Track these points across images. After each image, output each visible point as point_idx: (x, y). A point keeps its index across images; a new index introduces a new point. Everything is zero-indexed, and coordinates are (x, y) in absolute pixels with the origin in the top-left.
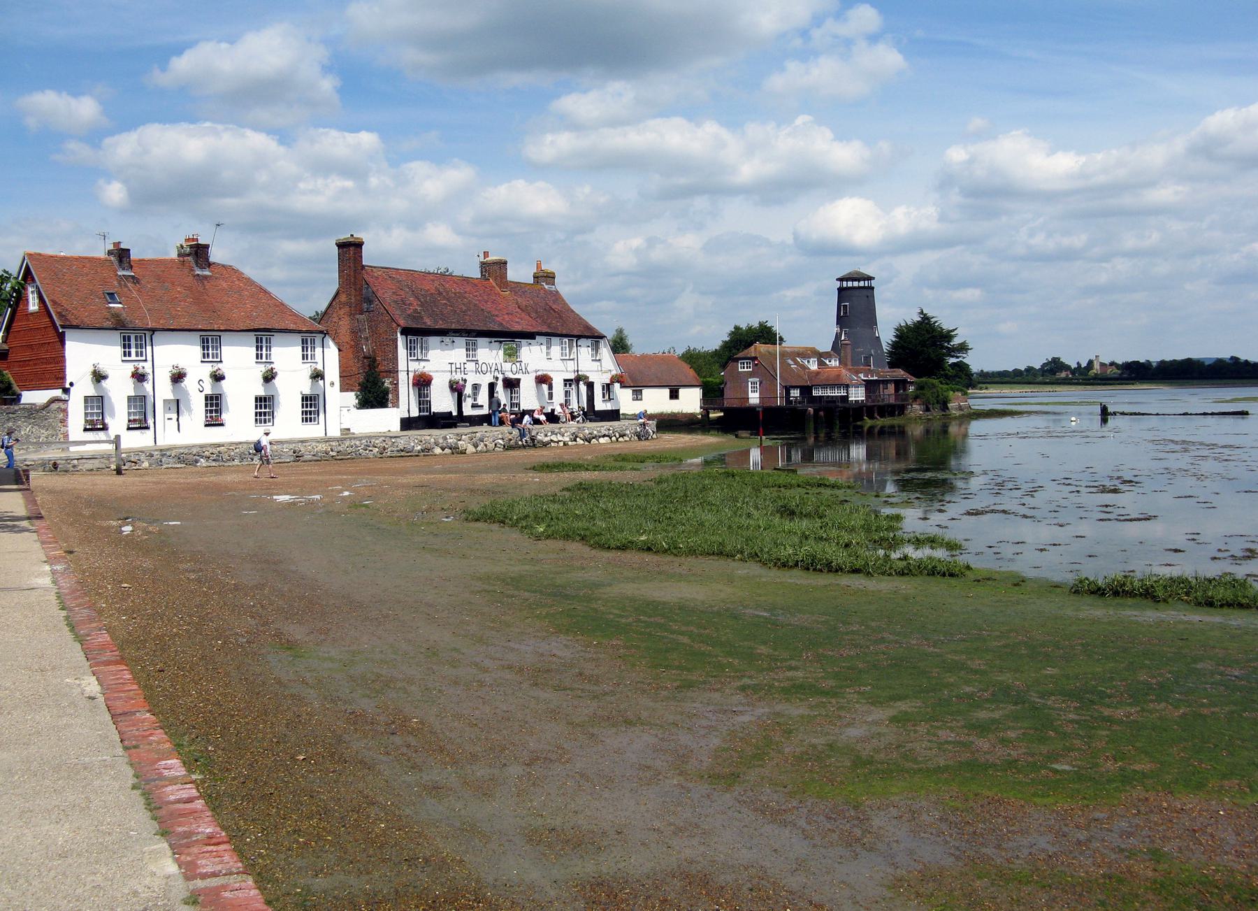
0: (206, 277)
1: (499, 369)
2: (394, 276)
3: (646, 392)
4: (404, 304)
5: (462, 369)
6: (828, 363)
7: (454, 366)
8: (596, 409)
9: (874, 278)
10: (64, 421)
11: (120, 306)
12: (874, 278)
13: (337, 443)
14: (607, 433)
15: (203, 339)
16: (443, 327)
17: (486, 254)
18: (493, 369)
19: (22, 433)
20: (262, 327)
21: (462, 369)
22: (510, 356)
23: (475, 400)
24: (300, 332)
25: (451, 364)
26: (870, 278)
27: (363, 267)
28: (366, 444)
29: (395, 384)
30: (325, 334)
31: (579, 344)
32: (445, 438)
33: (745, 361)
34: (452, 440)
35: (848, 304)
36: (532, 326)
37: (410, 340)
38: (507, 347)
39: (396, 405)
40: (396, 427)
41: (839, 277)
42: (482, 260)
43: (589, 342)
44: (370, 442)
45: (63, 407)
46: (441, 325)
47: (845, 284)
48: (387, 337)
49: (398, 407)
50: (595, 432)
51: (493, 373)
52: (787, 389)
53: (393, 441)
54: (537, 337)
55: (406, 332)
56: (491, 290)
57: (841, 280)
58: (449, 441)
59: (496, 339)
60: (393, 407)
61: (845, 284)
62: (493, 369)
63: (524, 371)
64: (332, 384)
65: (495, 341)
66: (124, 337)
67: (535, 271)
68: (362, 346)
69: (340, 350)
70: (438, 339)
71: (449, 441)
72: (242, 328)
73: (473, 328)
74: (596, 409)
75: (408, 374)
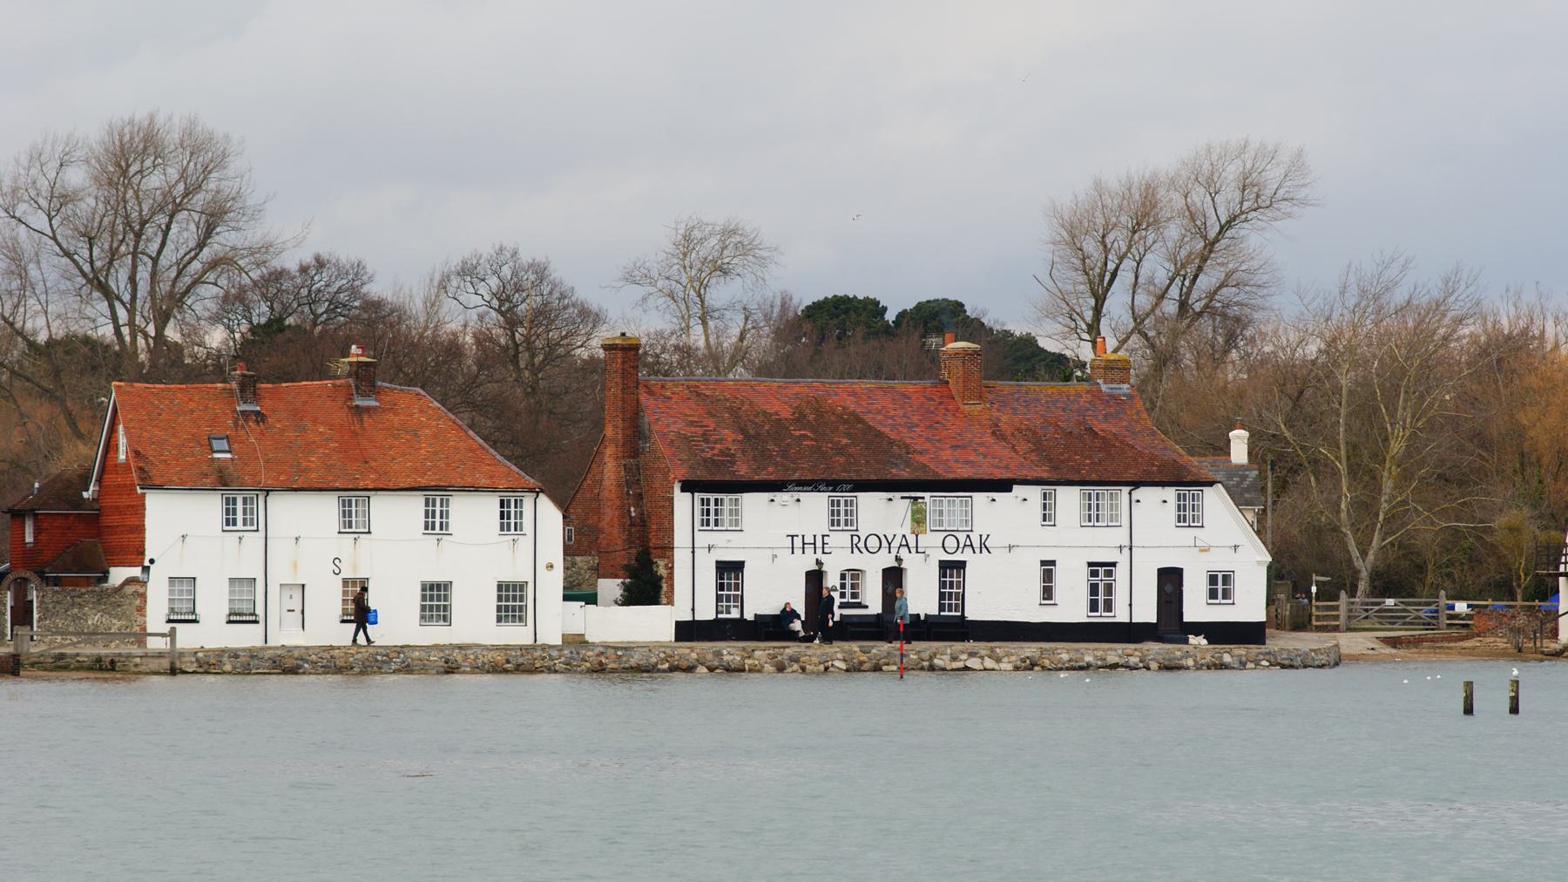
0: (368, 409)
1: (912, 544)
2: (708, 393)
4: (706, 441)
5: (819, 544)
10: (141, 610)
11: (228, 456)
14: (1121, 661)
15: (344, 501)
16: (772, 477)
18: (895, 544)
19: (90, 622)
20: (433, 483)
21: (819, 544)
22: (918, 523)
23: (854, 595)
24: (494, 490)
25: (792, 536)
28: (569, 655)
30: (538, 493)
32: (718, 654)
34: (732, 657)
36: (1007, 467)
39: (670, 602)
40: (669, 634)
43: (1170, 493)
44: (578, 653)
45: (141, 590)
49: (673, 605)
51: (894, 551)
53: (620, 653)
54: (1014, 486)
55: (688, 487)
58: (725, 658)
60: (668, 604)
62: (895, 544)
63: (976, 544)
65: (902, 498)
66: (227, 499)
68: (629, 508)
69: (564, 517)
71: (725, 658)
72: (402, 485)
73: (844, 476)
75: (693, 552)
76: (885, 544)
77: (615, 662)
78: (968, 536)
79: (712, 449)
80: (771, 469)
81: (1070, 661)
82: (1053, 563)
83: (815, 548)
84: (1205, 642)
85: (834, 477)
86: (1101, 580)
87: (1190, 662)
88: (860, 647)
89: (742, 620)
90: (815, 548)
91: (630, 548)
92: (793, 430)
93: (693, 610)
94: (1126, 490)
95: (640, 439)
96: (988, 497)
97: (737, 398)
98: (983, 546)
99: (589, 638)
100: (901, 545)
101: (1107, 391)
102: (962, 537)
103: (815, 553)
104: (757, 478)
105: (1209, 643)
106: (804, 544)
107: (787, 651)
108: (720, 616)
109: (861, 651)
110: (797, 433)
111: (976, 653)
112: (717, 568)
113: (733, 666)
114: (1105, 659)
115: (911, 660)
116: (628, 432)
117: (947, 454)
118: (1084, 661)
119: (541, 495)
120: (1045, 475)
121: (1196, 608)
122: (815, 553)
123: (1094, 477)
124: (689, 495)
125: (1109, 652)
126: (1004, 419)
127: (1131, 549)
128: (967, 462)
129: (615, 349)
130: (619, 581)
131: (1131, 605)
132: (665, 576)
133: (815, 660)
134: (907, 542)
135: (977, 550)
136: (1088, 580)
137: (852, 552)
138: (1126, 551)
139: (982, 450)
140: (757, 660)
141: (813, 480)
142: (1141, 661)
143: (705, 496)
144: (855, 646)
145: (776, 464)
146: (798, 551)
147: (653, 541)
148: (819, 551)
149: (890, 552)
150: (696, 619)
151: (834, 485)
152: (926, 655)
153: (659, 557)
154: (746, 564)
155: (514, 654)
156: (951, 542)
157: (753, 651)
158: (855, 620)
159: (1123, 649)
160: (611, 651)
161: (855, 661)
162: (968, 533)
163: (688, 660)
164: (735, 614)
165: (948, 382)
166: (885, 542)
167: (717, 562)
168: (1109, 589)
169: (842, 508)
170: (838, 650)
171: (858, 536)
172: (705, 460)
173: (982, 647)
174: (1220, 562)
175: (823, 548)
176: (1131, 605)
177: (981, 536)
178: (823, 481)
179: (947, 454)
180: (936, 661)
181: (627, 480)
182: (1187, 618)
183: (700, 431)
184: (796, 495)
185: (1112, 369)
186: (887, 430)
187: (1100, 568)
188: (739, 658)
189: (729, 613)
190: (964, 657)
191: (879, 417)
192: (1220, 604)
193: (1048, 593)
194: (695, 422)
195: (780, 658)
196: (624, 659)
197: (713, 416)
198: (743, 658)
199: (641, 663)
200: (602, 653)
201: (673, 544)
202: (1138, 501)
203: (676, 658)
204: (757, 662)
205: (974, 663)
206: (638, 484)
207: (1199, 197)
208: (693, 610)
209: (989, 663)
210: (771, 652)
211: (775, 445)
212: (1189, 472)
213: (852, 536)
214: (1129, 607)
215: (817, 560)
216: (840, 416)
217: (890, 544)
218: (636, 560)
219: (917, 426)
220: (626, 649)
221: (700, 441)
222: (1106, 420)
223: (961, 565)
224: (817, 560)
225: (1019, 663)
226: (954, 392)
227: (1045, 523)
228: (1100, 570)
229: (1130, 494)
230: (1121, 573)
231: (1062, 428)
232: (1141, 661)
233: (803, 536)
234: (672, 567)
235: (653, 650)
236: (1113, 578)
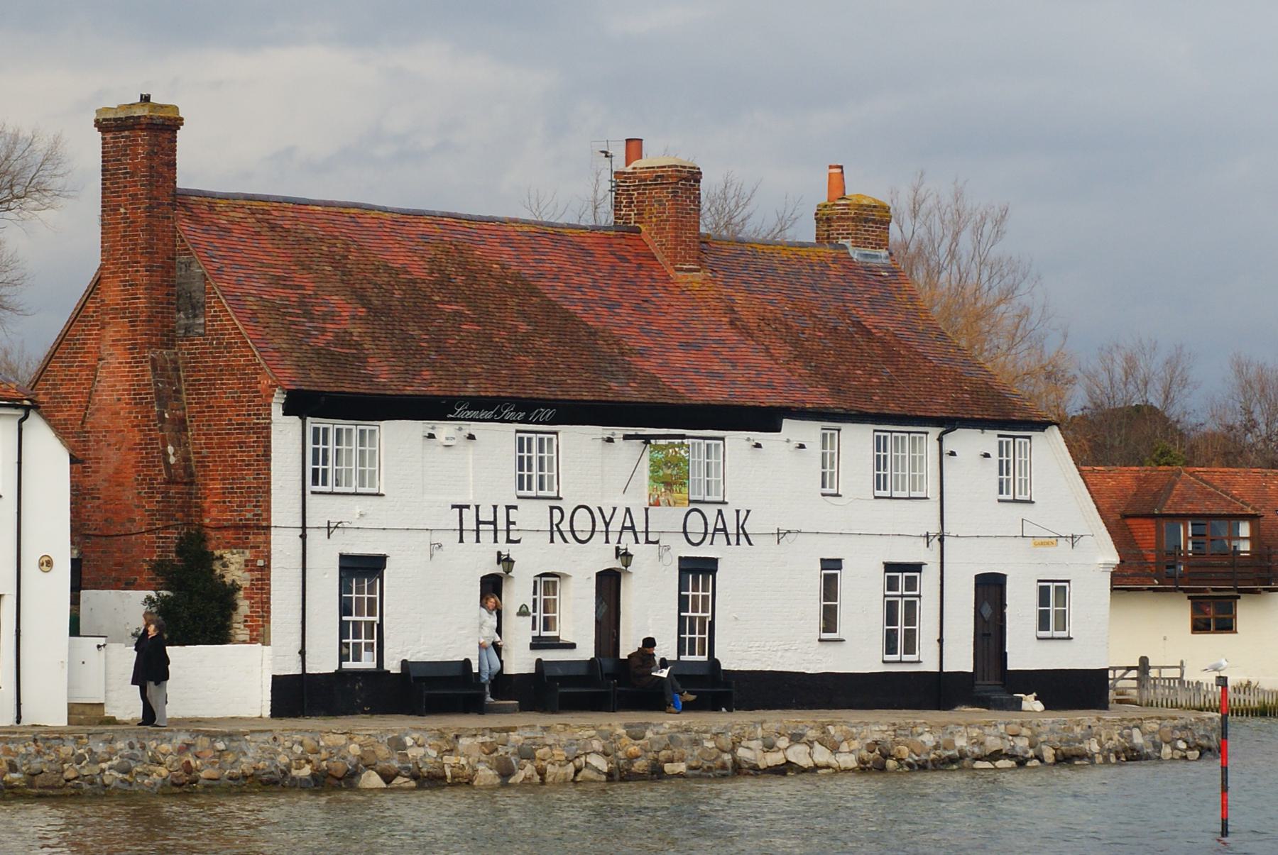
1: (640, 527)
4: (310, 316)
5: (502, 524)
7: (469, 515)
13: (32, 749)
14: (1006, 746)
16: (434, 390)
18: (616, 526)
21: (502, 524)
22: (668, 484)
23: (548, 624)
25: (461, 507)
27: (182, 200)
28: (127, 752)
29: (261, 569)
30: (27, 409)
31: (947, 449)
32: (398, 745)
34: (421, 751)
36: (770, 386)
37: (316, 430)
39: (260, 635)
40: (259, 702)
42: (620, 164)
43: (988, 440)
44: (143, 747)
46: (426, 384)
48: (241, 419)
49: (266, 643)
50: (961, 742)
51: (613, 538)
53: (220, 745)
55: (298, 405)
56: (640, 266)
58: (413, 753)
59: (631, 431)
60: (253, 640)
62: (616, 526)
63: (732, 529)
64: (47, 563)
65: (626, 437)
67: (824, 200)
68: (165, 446)
69: (73, 460)
70: (412, 430)
71: (413, 753)
73: (542, 392)
75: (303, 537)
76: (600, 525)
77: (213, 764)
78: (720, 512)
79: (323, 331)
80: (427, 374)
81: (936, 747)
83: (496, 531)
84: (1039, 706)
86: (902, 596)
87: (1095, 747)
88: (626, 726)
89: (379, 675)
90: (496, 531)
91: (167, 527)
92: (442, 302)
93: (302, 653)
94: (934, 432)
95: (179, 311)
96: (748, 439)
97: (336, 238)
98: (741, 531)
99: (117, 718)
100: (624, 528)
101: (861, 259)
102: (711, 512)
103: (496, 541)
104: (409, 390)
105: (1047, 707)
106: (479, 522)
107: (514, 737)
108: (349, 665)
109: (628, 733)
111: (802, 736)
112: (341, 568)
113: (424, 770)
114: (982, 744)
115: (705, 749)
116: (158, 295)
118: (955, 747)
119: (32, 414)
120: (830, 403)
122: (496, 541)
123: (893, 408)
124: (295, 420)
125: (987, 730)
126: (739, 298)
127: (941, 540)
128: (714, 374)
129: (131, 128)
130: (143, 594)
131: (941, 641)
132: (247, 584)
133: (560, 754)
134: (632, 522)
135: (733, 539)
136: (885, 596)
137: (552, 541)
138: (935, 543)
140: (463, 755)
141: (498, 397)
142: (1031, 746)
143: (322, 423)
144: (616, 723)
145: (432, 364)
146: (469, 537)
147: (214, 512)
148: (502, 536)
149: (607, 542)
150: (307, 671)
152: (726, 741)
153: (228, 546)
154: (389, 563)
155: (23, 750)
156: (695, 523)
157: (457, 737)
158: (560, 672)
159: (1007, 724)
160: (203, 742)
161: (620, 754)
162: (720, 507)
163: (344, 758)
164: (367, 662)
165: (638, 231)
166: (601, 520)
167: (343, 557)
168: (911, 608)
170: (593, 732)
171: (560, 509)
172: (318, 352)
174: (1055, 564)
175: (508, 531)
176: (941, 641)
177: (738, 511)
178: (512, 400)
179: (678, 358)
180: (742, 753)
181: (158, 391)
182: (1013, 664)
183: (294, 296)
184: (473, 427)
185: (866, 221)
186: (578, 309)
187: (900, 574)
188: (433, 753)
189: (357, 658)
190: (783, 742)
191: (560, 286)
192: (1052, 638)
193: (830, 619)
194: (279, 278)
195: (502, 751)
196: (230, 758)
198: (442, 753)
199: (261, 765)
200: (188, 746)
201: (269, 519)
202: (953, 454)
203: (324, 754)
204: (463, 761)
205: (799, 755)
206: (177, 399)
208: (302, 653)
209: (822, 755)
210: (487, 739)
211: (420, 328)
213: (552, 508)
214: (937, 645)
215: (499, 554)
217: (607, 525)
218: (178, 553)
219: (620, 306)
220: (230, 736)
221: (298, 316)
224: (499, 554)
226: (654, 248)
227: (881, 493)
229: (940, 440)
230: (927, 582)
231: (821, 320)
232: (1031, 746)
233: (477, 507)
234: (267, 567)
235: (281, 739)
236: (917, 593)
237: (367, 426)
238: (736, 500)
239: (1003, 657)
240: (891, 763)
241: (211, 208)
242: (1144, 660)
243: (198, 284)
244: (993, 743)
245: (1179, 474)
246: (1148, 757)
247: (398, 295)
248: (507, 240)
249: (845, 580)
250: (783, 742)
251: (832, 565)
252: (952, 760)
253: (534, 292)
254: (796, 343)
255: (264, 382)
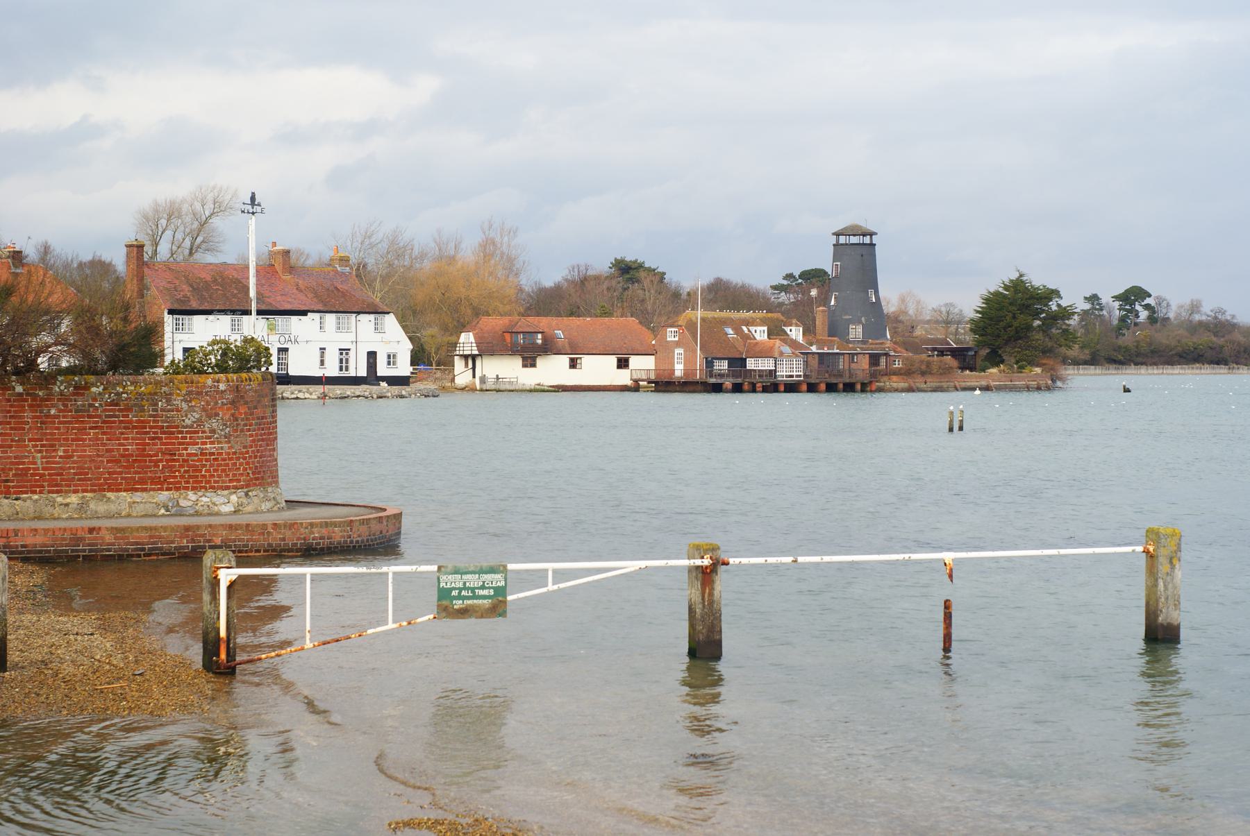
1: (266, 340)
2: (173, 268)
3: (586, 360)
6: (789, 332)
8: (378, 375)
9: (876, 234)
12: (876, 234)
14: (362, 394)
16: (206, 308)
17: (274, 244)
26: (871, 234)
33: (673, 329)
35: (839, 263)
36: (305, 304)
38: (269, 323)
41: (834, 232)
43: (372, 317)
46: (206, 307)
47: (842, 240)
52: (709, 364)
54: (309, 314)
55: (171, 312)
57: (837, 234)
59: (264, 317)
61: (842, 240)
63: (293, 340)
73: (238, 308)
74: (378, 375)
80: (206, 304)
82: (324, 349)
84: (386, 385)
85: (234, 308)
87: (390, 395)
98: (296, 341)
102: (287, 336)
104: (201, 308)
105: (389, 385)
110: (215, 287)
117: (279, 298)
120: (322, 309)
121: (382, 370)
123: (341, 309)
126: (300, 282)
128: (289, 302)
139: (293, 296)
143: (178, 316)
145: (208, 302)
151: (233, 312)
156: (282, 339)
168: (347, 360)
169: (236, 323)
173: (303, 387)
178: (228, 310)
179: (279, 298)
180: (284, 394)
190: (296, 392)
193: (322, 363)
197: (178, 279)
205: (301, 395)
207: (198, 206)
209: (307, 395)
212: (380, 308)
216: (231, 280)
219: (264, 285)
222: (342, 284)
223: (286, 350)
225: (319, 395)
228: (344, 351)
230: (352, 353)
237: (190, 317)
238: (294, 333)
239: (376, 372)
240: (327, 398)
241: (154, 265)
242: (497, 376)
243: (149, 284)
244: (358, 393)
245: (520, 319)
246: (406, 397)
247: (202, 284)
248: (235, 269)
249: (327, 352)
250: (296, 392)
251: (323, 349)
252: (345, 397)
253: (241, 283)
254: (316, 293)
255: (163, 307)
